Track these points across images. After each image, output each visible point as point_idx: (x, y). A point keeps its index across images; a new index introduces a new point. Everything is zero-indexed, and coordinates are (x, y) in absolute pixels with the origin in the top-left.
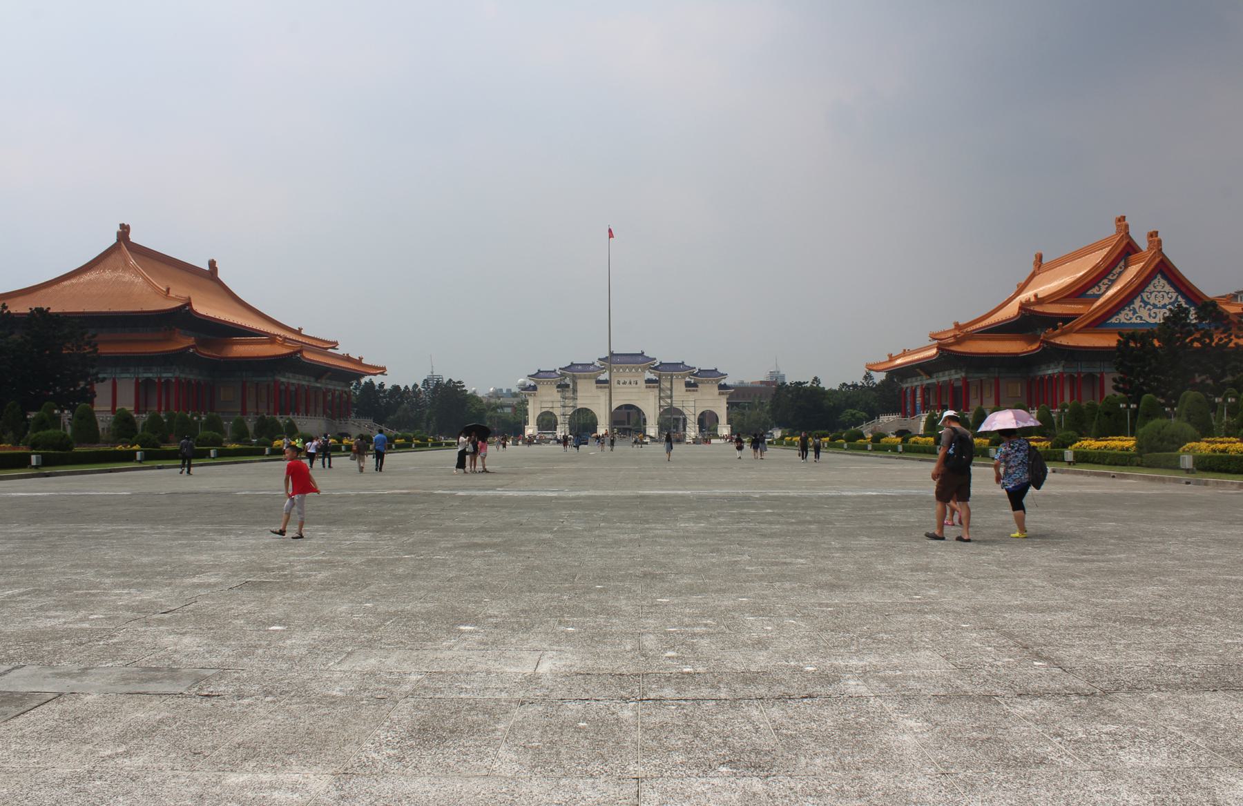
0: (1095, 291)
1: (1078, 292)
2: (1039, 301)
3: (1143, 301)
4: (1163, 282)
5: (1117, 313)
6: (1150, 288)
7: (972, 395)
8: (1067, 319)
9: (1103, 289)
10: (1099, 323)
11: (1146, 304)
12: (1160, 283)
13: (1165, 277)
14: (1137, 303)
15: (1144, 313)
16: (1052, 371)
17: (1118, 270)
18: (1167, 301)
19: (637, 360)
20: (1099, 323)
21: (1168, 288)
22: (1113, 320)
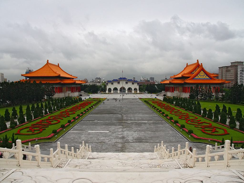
0: (193, 72)
1: (191, 72)
2: (185, 74)
3: (199, 75)
4: (203, 72)
5: (196, 77)
6: (201, 73)
7: (175, 89)
8: (188, 77)
9: (195, 72)
10: (193, 78)
11: (200, 75)
12: (202, 72)
13: (203, 71)
14: (199, 75)
15: (200, 77)
16: (186, 86)
17: (197, 69)
18: (203, 75)
19: (124, 79)
20: (193, 78)
21: (203, 73)
22: (195, 78)
